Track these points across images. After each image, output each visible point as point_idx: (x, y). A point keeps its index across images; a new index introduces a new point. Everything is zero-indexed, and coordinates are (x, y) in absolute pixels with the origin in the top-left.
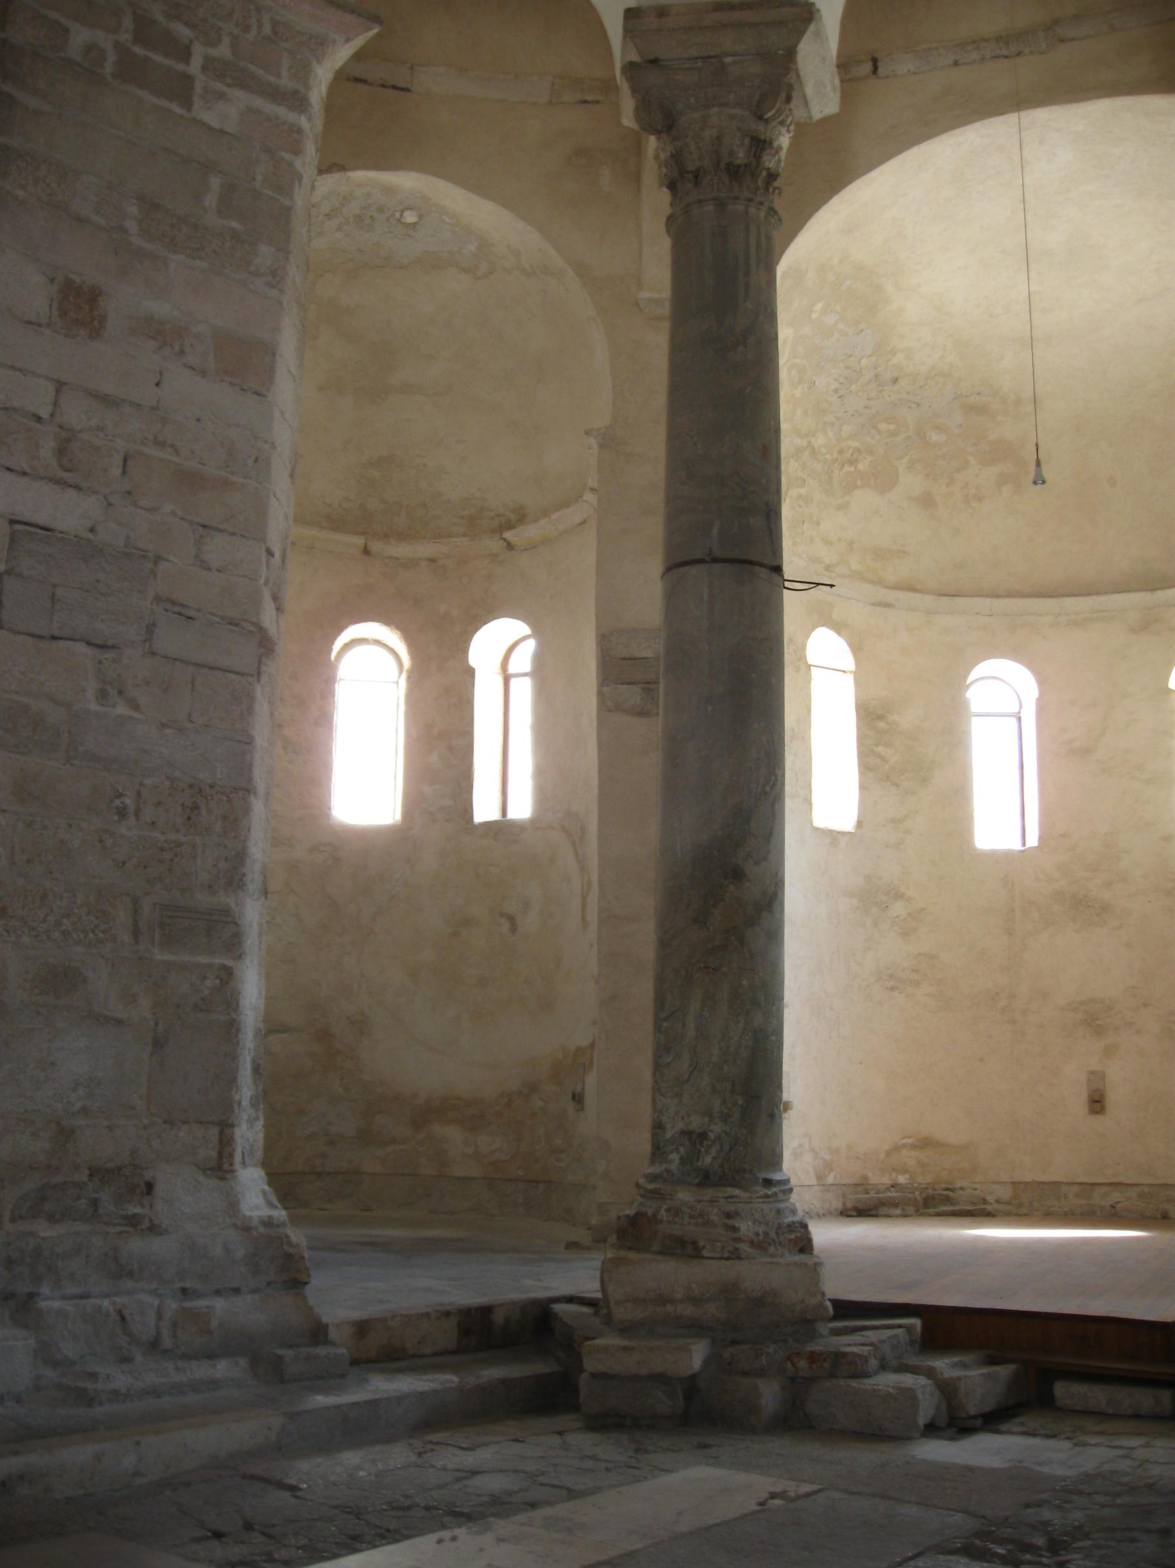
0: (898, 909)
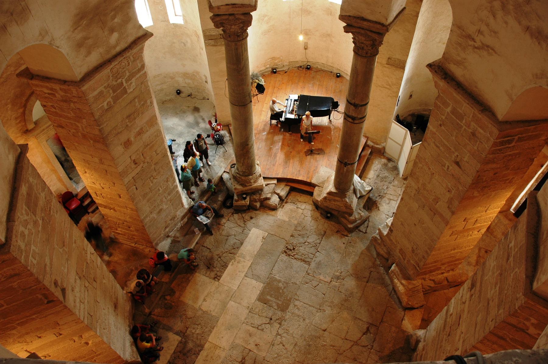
0: (266, 18)
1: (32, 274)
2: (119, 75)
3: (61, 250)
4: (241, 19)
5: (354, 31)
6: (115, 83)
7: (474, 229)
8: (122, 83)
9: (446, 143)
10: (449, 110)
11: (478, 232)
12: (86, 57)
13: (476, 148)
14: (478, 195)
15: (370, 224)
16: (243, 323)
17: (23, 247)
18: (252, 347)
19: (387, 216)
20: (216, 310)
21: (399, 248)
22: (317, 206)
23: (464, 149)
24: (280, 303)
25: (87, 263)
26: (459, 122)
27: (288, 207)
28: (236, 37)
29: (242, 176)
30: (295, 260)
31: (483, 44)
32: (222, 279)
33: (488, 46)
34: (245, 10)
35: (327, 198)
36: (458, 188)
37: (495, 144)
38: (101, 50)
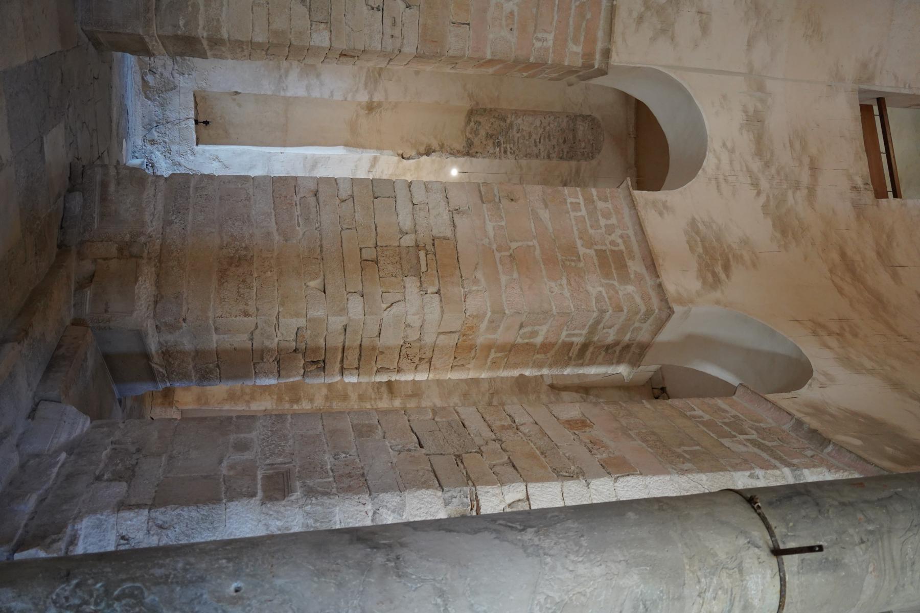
3: (514, 245)
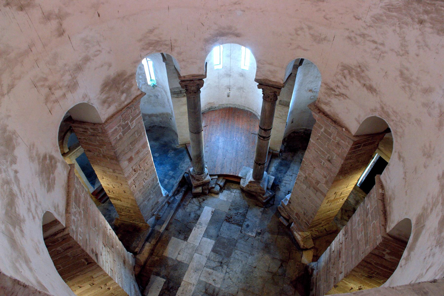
1: (80, 247)
2: (127, 118)
3: (94, 229)
4: (197, 83)
5: (263, 87)
6: (124, 123)
7: (340, 198)
8: (128, 123)
9: (322, 149)
10: (322, 130)
11: (343, 199)
12: (108, 108)
13: (340, 151)
14: (342, 178)
15: (276, 199)
16: (204, 267)
17: (74, 229)
18: (211, 282)
19: (285, 194)
20: (187, 260)
21: (295, 212)
22: (242, 190)
23: (333, 153)
24: (226, 252)
25: (108, 236)
26: (329, 137)
27: (225, 192)
28: (194, 93)
29: (197, 175)
30: (233, 225)
31: (340, 93)
32: (188, 239)
33: (343, 94)
34: (200, 78)
35: (249, 185)
36: (331, 175)
37: (351, 149)
38: (116, 104)
